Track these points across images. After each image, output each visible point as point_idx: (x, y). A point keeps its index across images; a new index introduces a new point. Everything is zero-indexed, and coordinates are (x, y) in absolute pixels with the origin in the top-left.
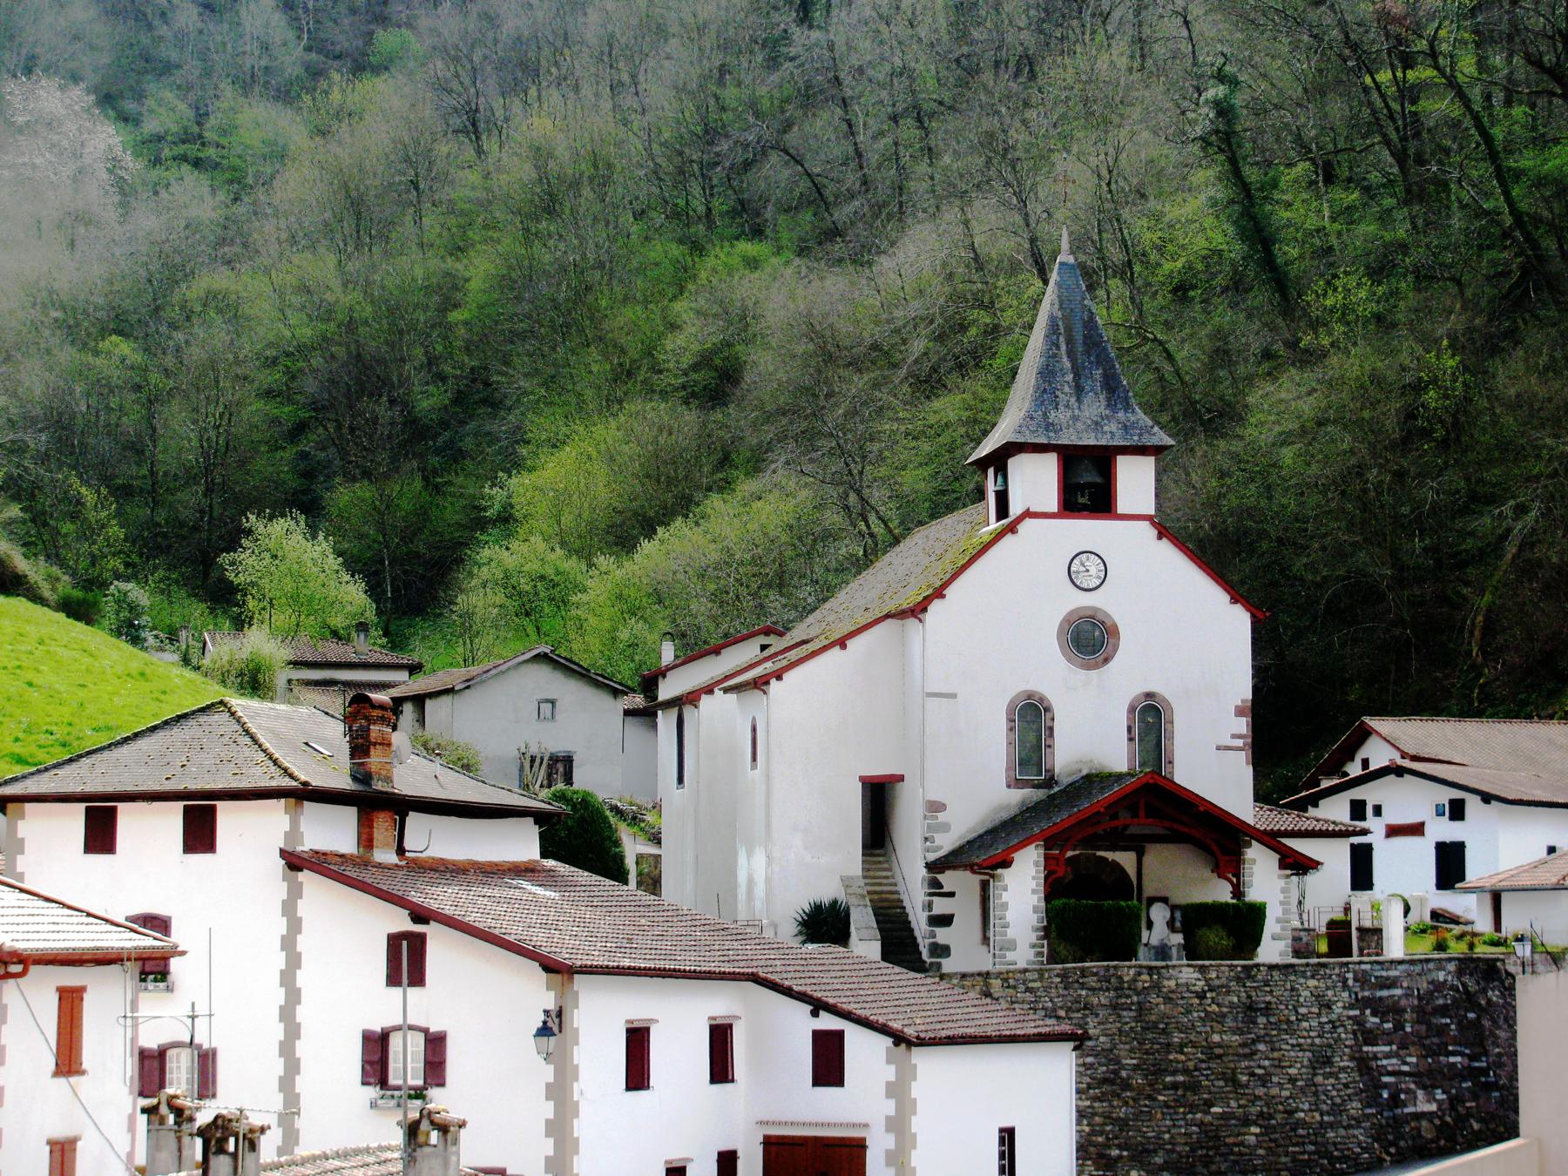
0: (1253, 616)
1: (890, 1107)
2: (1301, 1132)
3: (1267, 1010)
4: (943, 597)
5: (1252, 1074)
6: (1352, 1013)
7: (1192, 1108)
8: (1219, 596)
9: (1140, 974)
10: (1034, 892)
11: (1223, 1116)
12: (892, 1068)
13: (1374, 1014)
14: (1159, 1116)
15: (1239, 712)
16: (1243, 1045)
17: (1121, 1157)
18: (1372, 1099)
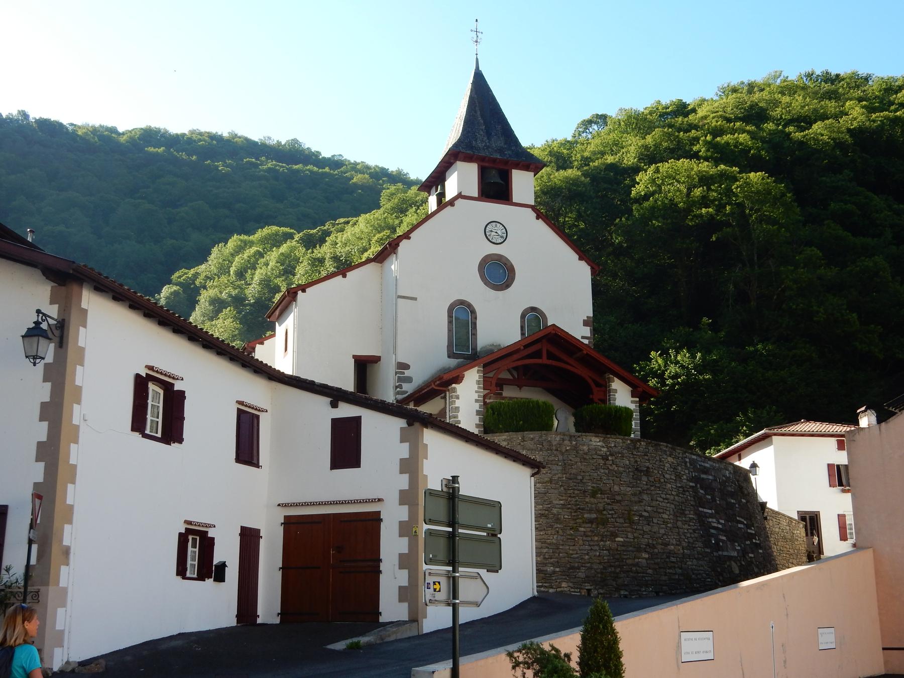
0: (592, 269)
1: (403, 482)
2: (673, 559)
3: (647, 472)
4: (409, 238)
5: (641, 516)
6: (691, 484)
7: (603, 538)
8: (572, 256)
9: (563, 440)
10: (477, 401)
11: (623, 544)
12: (406, 445)
13: (702, 488)
14: (581, 542)
15: (586, 323)
16: (634, 495)
17: (554, 572)
18: (707, 544)
